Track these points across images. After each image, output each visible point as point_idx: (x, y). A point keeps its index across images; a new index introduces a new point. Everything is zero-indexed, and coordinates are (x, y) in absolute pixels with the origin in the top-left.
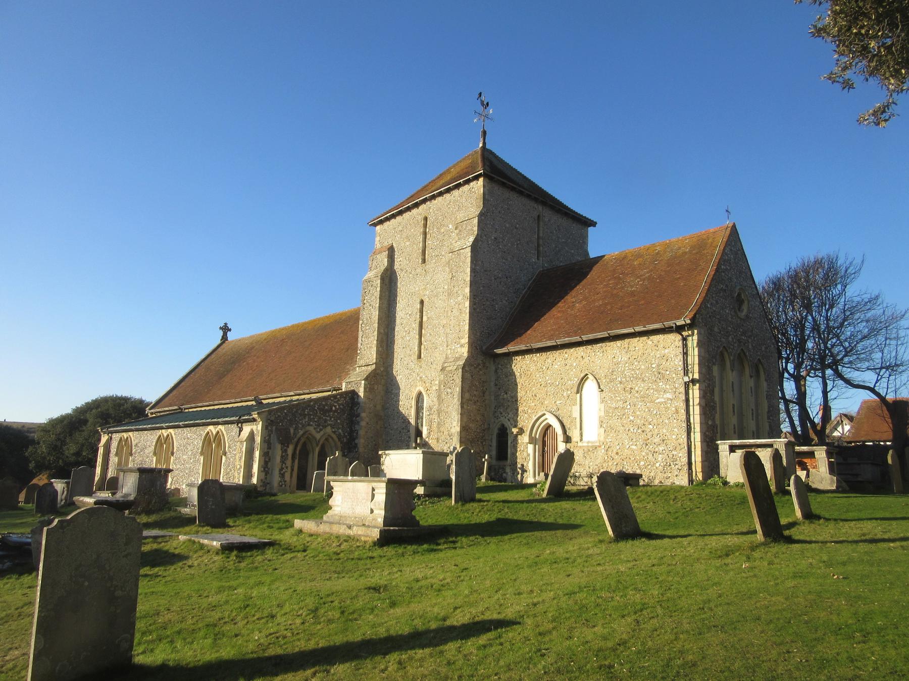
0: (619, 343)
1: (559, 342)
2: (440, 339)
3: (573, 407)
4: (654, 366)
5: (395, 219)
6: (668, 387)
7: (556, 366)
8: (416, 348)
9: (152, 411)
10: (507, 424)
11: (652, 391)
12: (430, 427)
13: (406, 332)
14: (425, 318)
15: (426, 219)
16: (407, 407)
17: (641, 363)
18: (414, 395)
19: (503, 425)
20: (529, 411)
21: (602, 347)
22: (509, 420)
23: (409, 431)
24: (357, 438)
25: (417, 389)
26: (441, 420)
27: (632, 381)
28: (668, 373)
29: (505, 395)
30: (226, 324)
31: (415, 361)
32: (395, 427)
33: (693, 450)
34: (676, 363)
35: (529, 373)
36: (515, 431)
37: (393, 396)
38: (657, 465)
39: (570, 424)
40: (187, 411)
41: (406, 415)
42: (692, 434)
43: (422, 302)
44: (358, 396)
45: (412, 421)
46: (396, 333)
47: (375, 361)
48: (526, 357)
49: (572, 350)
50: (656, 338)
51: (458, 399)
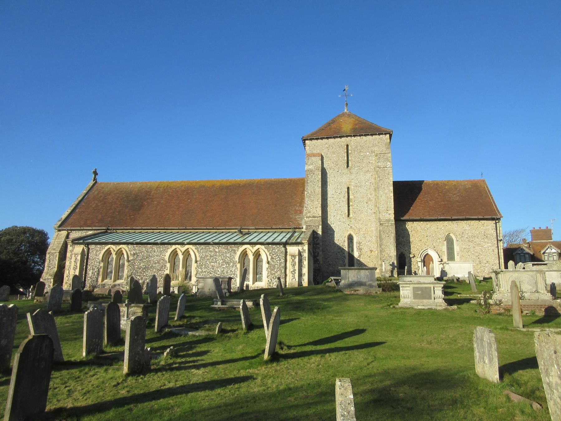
0: (465, 222)
1: (439, 218)
2: (364, 209)
5: (322, 140)
6: (489, 241)
8: (347, 212)
9: (61, 228)
10: (406, 253)
12: (361, 252)
14: (351, 197)
15: (347, 146)
16: (340, 240)
18: (347, 235)
19: (402, 253)
21: (457, 222)
23: (344, 254)
24: (317, 256)
25: (349, 233)
26: (382, 249)
29: (402, 240)
31: (347, 218)
33: (501, 266)
35: (417, 230)
36: (411, 256)
38: (486, 271)
40: (115, 231)
41: (341, 245)
42: (500, 260)
43: (348, 188)
44: (317, 234)
45: (346, 249)
46: (328, 202)
47: (321, 215)
48: (414, 222)
49: (441, 222)
50: (483, 222)
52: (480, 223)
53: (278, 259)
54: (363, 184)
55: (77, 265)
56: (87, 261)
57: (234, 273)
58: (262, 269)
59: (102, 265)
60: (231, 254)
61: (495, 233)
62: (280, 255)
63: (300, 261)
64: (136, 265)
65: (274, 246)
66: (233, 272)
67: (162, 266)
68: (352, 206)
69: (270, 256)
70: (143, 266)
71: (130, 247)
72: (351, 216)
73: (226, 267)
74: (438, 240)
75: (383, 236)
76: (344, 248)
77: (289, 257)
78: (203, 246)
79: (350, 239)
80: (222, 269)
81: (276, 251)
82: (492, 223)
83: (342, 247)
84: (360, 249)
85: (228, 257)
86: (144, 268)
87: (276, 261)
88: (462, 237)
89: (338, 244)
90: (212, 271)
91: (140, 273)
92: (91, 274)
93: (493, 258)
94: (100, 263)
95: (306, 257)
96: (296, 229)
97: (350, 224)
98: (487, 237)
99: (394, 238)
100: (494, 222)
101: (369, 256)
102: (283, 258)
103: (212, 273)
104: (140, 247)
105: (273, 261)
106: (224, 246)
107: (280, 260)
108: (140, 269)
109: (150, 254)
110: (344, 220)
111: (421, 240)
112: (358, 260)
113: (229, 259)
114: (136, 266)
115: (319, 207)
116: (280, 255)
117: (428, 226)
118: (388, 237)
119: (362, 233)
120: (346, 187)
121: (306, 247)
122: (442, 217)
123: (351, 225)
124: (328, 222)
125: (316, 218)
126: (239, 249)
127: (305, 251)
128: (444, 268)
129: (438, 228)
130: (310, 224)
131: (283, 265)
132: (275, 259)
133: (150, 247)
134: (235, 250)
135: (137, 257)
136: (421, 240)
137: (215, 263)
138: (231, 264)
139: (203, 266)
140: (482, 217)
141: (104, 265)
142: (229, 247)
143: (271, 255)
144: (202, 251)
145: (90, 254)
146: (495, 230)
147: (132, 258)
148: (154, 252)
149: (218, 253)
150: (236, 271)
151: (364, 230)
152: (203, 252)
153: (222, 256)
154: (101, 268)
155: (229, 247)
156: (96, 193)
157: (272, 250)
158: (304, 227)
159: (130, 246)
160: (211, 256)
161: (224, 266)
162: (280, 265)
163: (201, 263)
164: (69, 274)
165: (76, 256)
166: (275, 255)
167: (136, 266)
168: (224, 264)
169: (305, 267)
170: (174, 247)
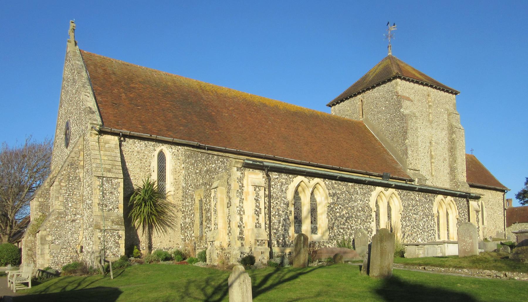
53: (463, 214)
54: (440, 142)
59: (292, 208)
60: (429, 205)
70: (346, 214)
71: (327, 183)
77: (473, 214)
81: (462, 204)
90: (415, 226)
92: (277, 224)
94: (288, 205)
102: (466, 213)
104: (340, 184)
107: (464, 215)
109: (353, 197)
113: (428, 211)
114: (338, 214)
135: (337, 200)
138: (430, 217)
139: (407, 218)
145: (271, 189)
147: (332, 201)
154: (291, 213)
155: (427, 196)
160: (413, 206)
163: (405, 214)
164: (242, 222)
165: (257, 189)
167: (338, 214)
168: (424, 216)
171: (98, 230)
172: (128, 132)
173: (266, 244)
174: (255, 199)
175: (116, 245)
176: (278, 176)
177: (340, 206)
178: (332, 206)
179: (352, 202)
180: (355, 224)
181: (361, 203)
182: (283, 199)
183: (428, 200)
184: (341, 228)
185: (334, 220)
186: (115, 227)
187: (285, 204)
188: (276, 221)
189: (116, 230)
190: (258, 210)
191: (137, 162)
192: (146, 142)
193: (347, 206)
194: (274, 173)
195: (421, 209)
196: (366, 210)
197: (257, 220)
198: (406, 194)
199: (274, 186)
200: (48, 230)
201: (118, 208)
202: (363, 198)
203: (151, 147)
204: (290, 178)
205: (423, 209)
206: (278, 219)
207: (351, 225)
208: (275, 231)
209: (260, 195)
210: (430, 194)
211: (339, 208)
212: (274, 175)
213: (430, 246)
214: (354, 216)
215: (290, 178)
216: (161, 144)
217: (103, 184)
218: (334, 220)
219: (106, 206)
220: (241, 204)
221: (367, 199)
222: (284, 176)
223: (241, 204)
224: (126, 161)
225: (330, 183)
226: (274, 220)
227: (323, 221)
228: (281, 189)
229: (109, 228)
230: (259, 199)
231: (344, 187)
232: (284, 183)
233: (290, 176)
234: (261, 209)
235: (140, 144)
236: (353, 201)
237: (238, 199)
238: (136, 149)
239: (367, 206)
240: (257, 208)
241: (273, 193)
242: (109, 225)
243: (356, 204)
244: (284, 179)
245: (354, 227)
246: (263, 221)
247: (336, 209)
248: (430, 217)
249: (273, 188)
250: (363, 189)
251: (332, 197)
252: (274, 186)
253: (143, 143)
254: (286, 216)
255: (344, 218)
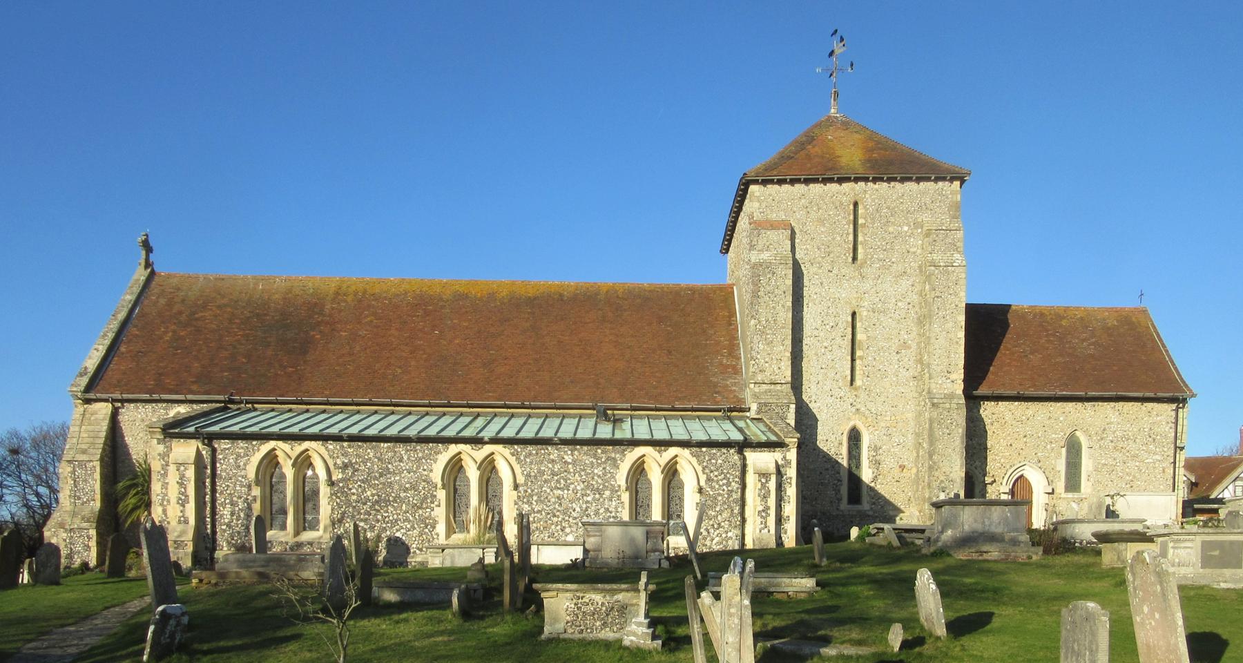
0: (1112, 404)
2: (892, 367)
3: (1058, 460)
4: (1145, 430)
7: (1039, 418)
8: (848, 372)
11: (1142, 452)
13: (826, 348)
14: (859, 337)
17: (1133, 426)
20: (1002, 461)
22: (976, 468)
23: (839, 473)
25: (851, 424)
26: (934, 463)
27: (1124, 441)
28: (1158, 437)
30: (147, 235)
31: (847, 389)
32: (812, 467)
34: (1167, 430)
35: (1004, 421)
37: (803, 427)
39: (1054, 476)
45: (845, 463)
46: (805, 348)
47: (789, 379)
49: (1059, 404)
50: (1150, 405)
51: (962, 443)
52: (1143, 408)
53: (725, 481)
55: (188, 493)
56: (213, 484)
57: (613, 514)
58: (682, 507)
59: (256, 491)
60: (604, 468)
61: (1173, 431)
62: (728, 473)
63: (779, 487)
64: (354, 494)
65: (714, 451)
66: (611, 512)
67: (425, 498)
68: (861, 358)
69: (704, 473)
71: (331, 447)
72: (858, 382)
73: (594, 499)
74: (1049, 447)
75: (938, 433)
76: (840, 461)
77: (751, 479)
78: (530, 448)
79: (854, 437)
80: (584, 506)
81: (720, 461)
82: (1168, 408)
83: (834, 457)
84: (876, 463)
85: (599, 476)
86: (377, 502)
87: (720, 486)
88: (1102, 439)
89: (825, 449)
90: (558, 511)
91: (365, 514)
93: (1162, 487)
94: (249, 487)
95: (791, 478)
96: (732, 411)
97: (855, 403)
98: (1154, 440)
99: (962, 437)
100: (1174, 406)
101: (897, 478)
102: (737, 480)
103: (558, 513)
105: (712, 488)
106: (585, 448)
107: (729, 484)
108: (365, 504)
109: (390, 466)
110: (842, 394)
111: (1011, 445)
112: (872, 489)
113: (600, 481)
114: (354, 497)
115: (786, 359)
116: (728, 473)
117: (1030, 412)
118: (949, 434)
119: (883, 424)
120: (849, 312)
121: (792, 455)
122: (1064, 393)
123: (858, 406)
124: (804, 397)
125: (778, 387)
126: (624, 456)
127: (789, 463)
128: (1113, 506)
129: (1050, 418)
130: (768, 401)
131: (736, 496)
132: (717, 482)
133: (388, 447)
134: (614, 459)
135: (353, 473)
136: (1011, 445)
137: (566, 491)
138: (607, 493)
140: (1151, 395)
141: (263, 492)
142: (599, 451)
143: (707, 471)
144: (528, 460)
145: (218, 465)
146: (1173, 425)
147: (340, 476)
148: (401, 461)
149: (570, 466)
150: (620, 509)
151: (888, 418)
152: (531, 463)
153: (583, 473)
156: (162, 301)
157: (710, 460)
158: (754, 407)
159: (331, 445)
160: (554, 474)
161: (589, 499)
162: (729, 496)
163: (529, 491)
164: (166, 515)
165: (182, 468)
166: (716, 473)
167: (354, 497)
169: (789, 502)
170: (454, 449)
171: (62, 530)
172: (117, 396)
173: (190, 546)
174: (178, 482)
175: (86, 548)
176: (230, 446)
177: (359, 483)
178: (341, 485)
179: (389, 476)
180: (394, 512)
181: (409, 475)
182: (240, 479)
183: (603, 460)
184: (361, 520)
185: (344, 507)
186: (85, 525)
187: (244, 486)
188: (225, 513)
189: (85, 529)
190: (183, 498)
191: (141, 435)
192: (154, 405)
193: (376, 482)
194: (222, 441)
195: (579, 479)
196: (421, 488)
197: (181, 512)
198: (534, 452)
199: (222, 461)
200: (53, 530)
201: (94, 500)
202: (415, 466)
203: (162, 411)
204: (254, 446)
205: (584, 477)
206: (230, 509)
207: (384, 514)
208: (224, 527)
209: (187, 476)
210: (611, 447)
211: (356, 486)
212: (222, 445)
213: (460, 550)
214: (391, 499)
215: (254, 446)
216: (176, 405)
217: (74, 471)
218: (344, 507)
219: (79, 498)
220: (163, 491)
221: (425, 467)
222: (241, 444)
223: (163, 491)
224: (125, 434)
225: (338, 447)
226: (225, 513)
227: (325, 509)
228: (235, 463)
229: (76, 526)
230: (185, 483)
231: (369, 451)
232: (242, 454)
233: (254, 443)
234: (188, 496)
235: (146, 409)
236: (390, 473)
237: (160, 484)
238: (139, 416)
239: (424, 481)
240: (181, 496)
241: (221, 471)
242: (77, 523)
243: (397, 478)
244: (242, 448)
245: (391, 518)
246: (192, 513)
247: (351, 489)
248: (607, 493)
249: (220, 463)
250: (416, 451)
251: (340, 470)
252: (222, 461)
253: (149, 406)
254: (246, 504)
255: (368, 503)
